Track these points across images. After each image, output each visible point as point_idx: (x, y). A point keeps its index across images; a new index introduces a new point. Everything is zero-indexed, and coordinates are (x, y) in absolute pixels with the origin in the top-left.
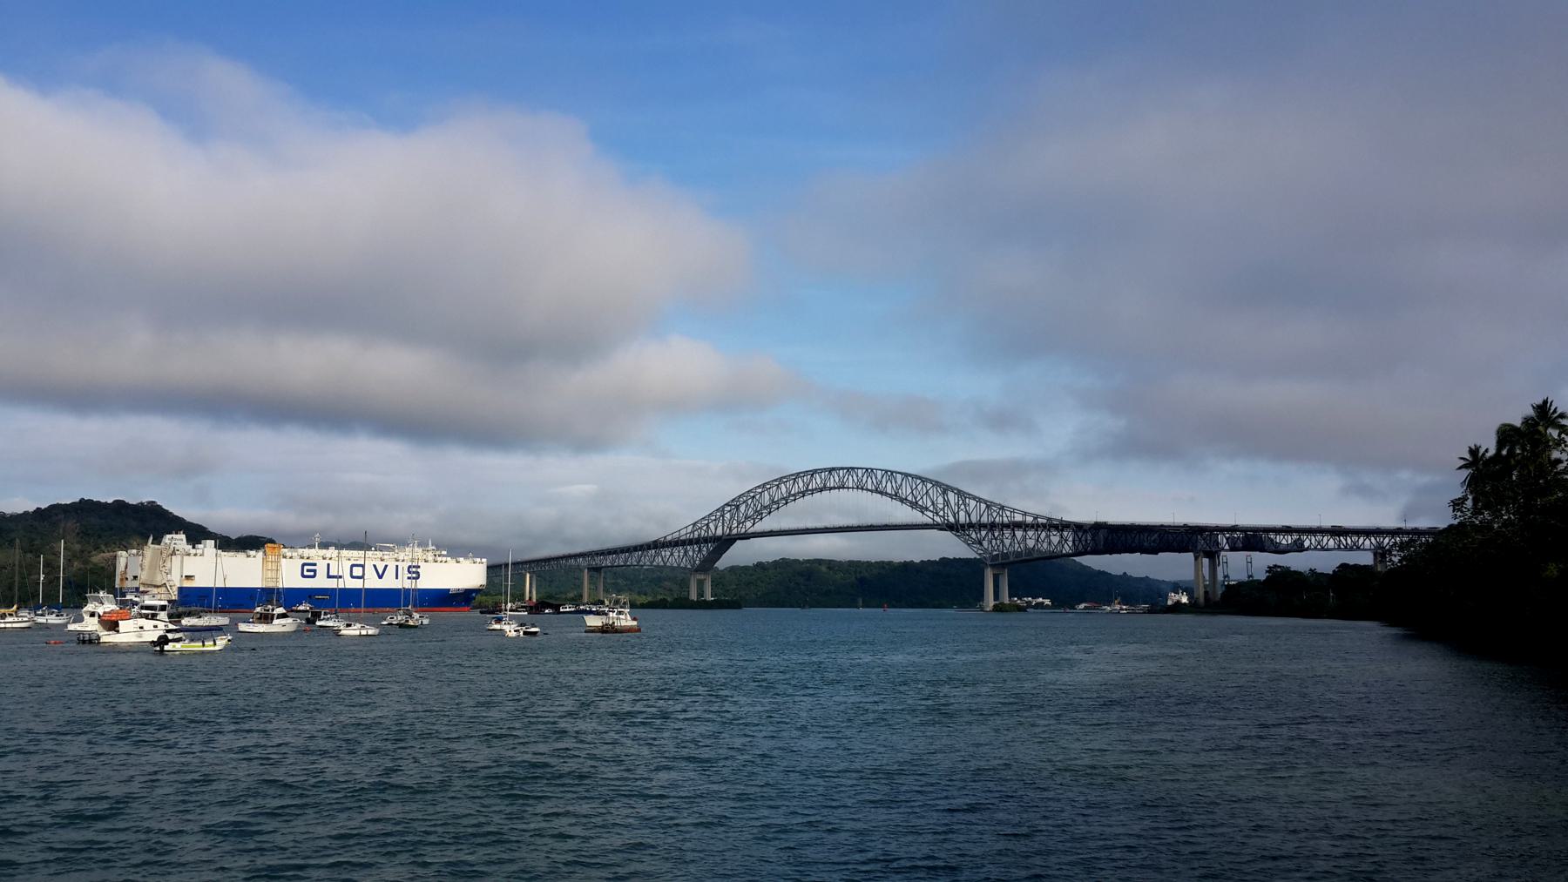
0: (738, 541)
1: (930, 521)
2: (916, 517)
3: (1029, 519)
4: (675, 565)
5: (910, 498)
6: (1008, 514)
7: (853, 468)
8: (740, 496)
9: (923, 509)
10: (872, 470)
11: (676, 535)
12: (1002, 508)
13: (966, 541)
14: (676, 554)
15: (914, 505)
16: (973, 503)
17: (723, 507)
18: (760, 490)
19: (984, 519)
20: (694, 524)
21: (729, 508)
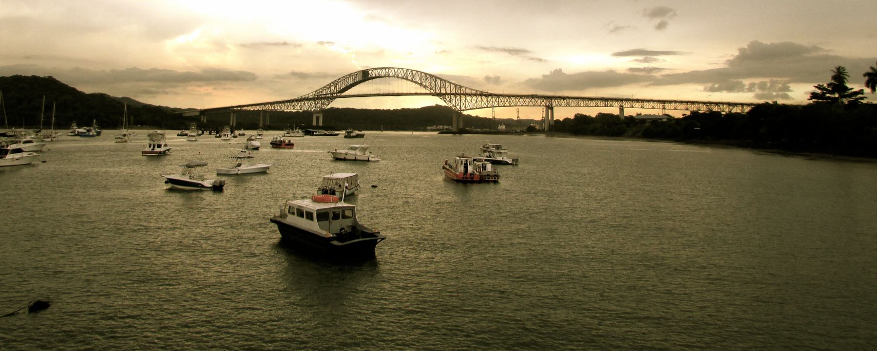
0: (336, 99)
1: (429, 92)
2: (423, 91)
3: (474, 92)
4: (306, 109)
5: (419, 82)
6: (464, 89)
7: (393, 68)
8: (339, 79)
9: (425, 87)
10: (402, 69)
11: (307, 96)
12: (461, 87)
13: (445, 101)
14: (306, 104)
15: (421, 84)
16: (447, 84)
17: (330, 84)
18: (348, 77)
19: (454, 92)
20: (316, 91)
21: (332, 84)
